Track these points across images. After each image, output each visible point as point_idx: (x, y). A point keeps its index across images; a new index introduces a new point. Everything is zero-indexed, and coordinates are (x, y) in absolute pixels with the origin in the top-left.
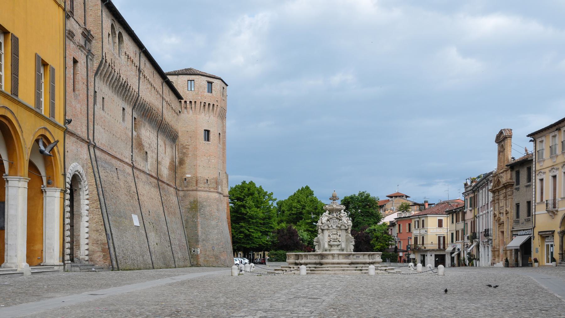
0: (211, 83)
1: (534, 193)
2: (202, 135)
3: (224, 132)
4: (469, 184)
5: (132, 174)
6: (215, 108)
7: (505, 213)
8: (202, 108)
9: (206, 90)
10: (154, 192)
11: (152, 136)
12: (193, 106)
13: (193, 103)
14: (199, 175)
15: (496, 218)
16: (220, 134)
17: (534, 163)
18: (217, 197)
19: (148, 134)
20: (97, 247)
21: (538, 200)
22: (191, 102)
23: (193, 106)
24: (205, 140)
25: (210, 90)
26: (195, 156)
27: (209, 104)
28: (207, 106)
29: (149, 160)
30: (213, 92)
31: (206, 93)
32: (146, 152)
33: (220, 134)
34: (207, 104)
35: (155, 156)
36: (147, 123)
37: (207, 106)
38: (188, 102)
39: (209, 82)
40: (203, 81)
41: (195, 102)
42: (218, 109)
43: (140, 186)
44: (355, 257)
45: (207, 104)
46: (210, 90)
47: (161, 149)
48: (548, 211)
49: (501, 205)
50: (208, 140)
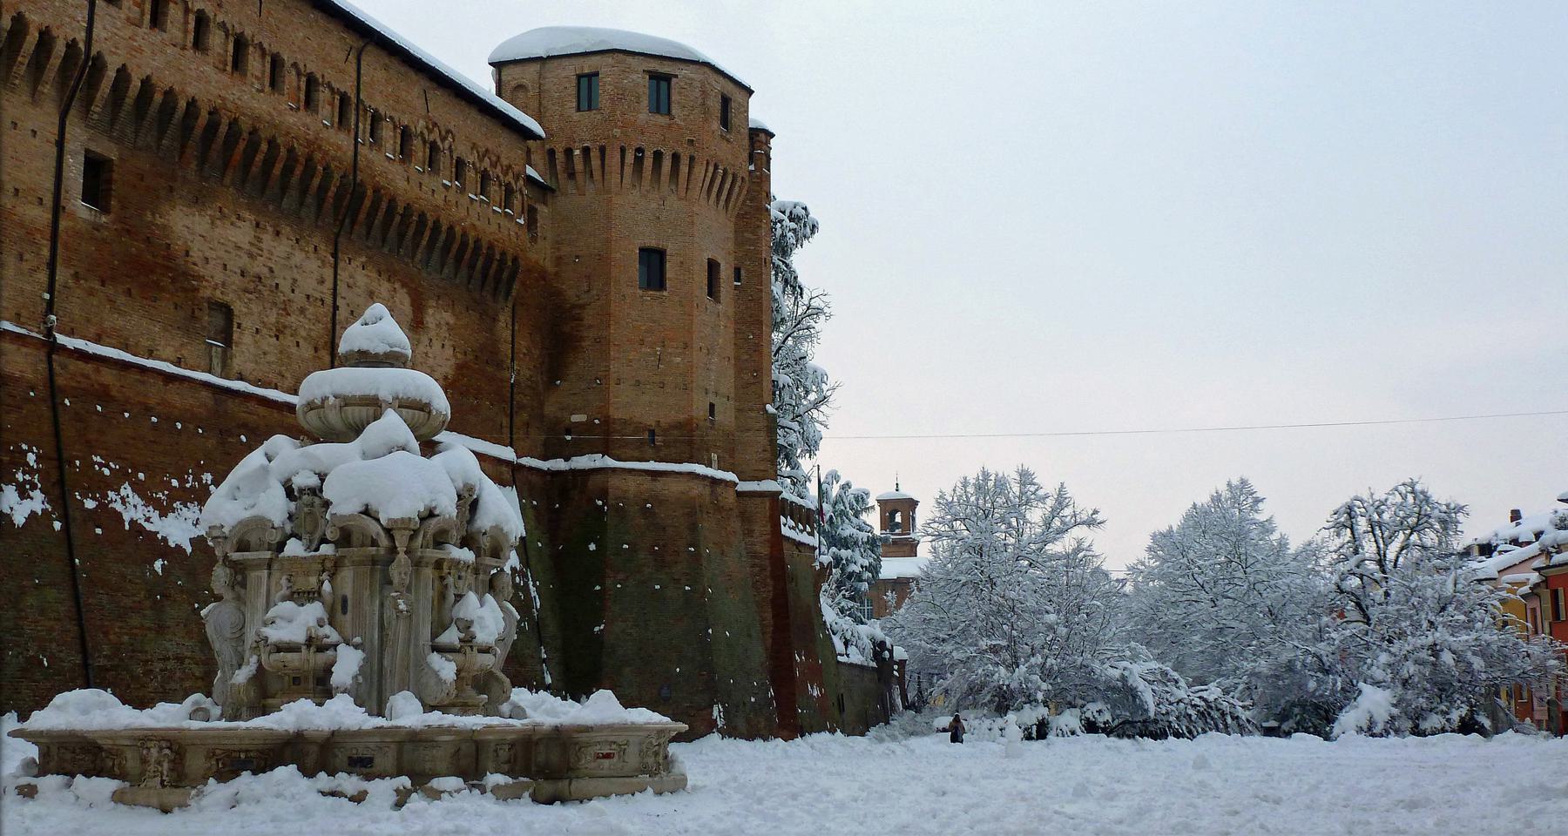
0: (667, 78)
6: (684, 169)
8: (628, 170)
9: (645, 102)
12: (596, 163)
13: (595, 154)
14: (616, 414)
16: (713, 266)
18: (695, 492)
22: (586, 151)
23: (596, 163)
26: (603, 343)
27: (658, 156)
28: (648, 162)
31: (644, 116)
32: (227, 311)
33: (713, 266)
34: (649, 155)
37: (648, 162)
38: (577, 152)
39: (656, 77)
41: (602, 150)
42: (699, 170)
45: (649, 155)
50: (661, 286)
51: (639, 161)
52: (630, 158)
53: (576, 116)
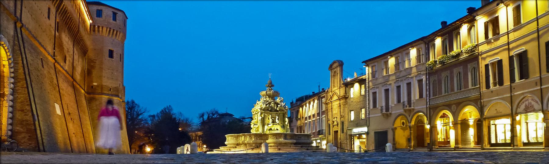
1: (368, 102)
2: (107, 54)
3: (123, 54)
4: (294, 102)
5: (54, 68)
7: (339, 117)
8: (108, 32)
10: (70, 90)
11: (70, 42)
15: (330, 122)
17: (367, 81)
19: (67, 39)
20: (22, 127)
21: (371, 107)
22: (99, 27)
24: (109, 57)
25: (115, 19)
29: (67, 62)
30: (117, 21)
31: (112, 21)
35: (71, 61)
36: (66, 30)
37: (112, 31)
40: (110, 12)
43: (60, 82)
44: (297, 138)
46: (115, 19)
47: (76, 57)
48: (383, 115)
49: (334, 112)
51: (110, 30)
52: (108, 30)
53: (97, 18)
